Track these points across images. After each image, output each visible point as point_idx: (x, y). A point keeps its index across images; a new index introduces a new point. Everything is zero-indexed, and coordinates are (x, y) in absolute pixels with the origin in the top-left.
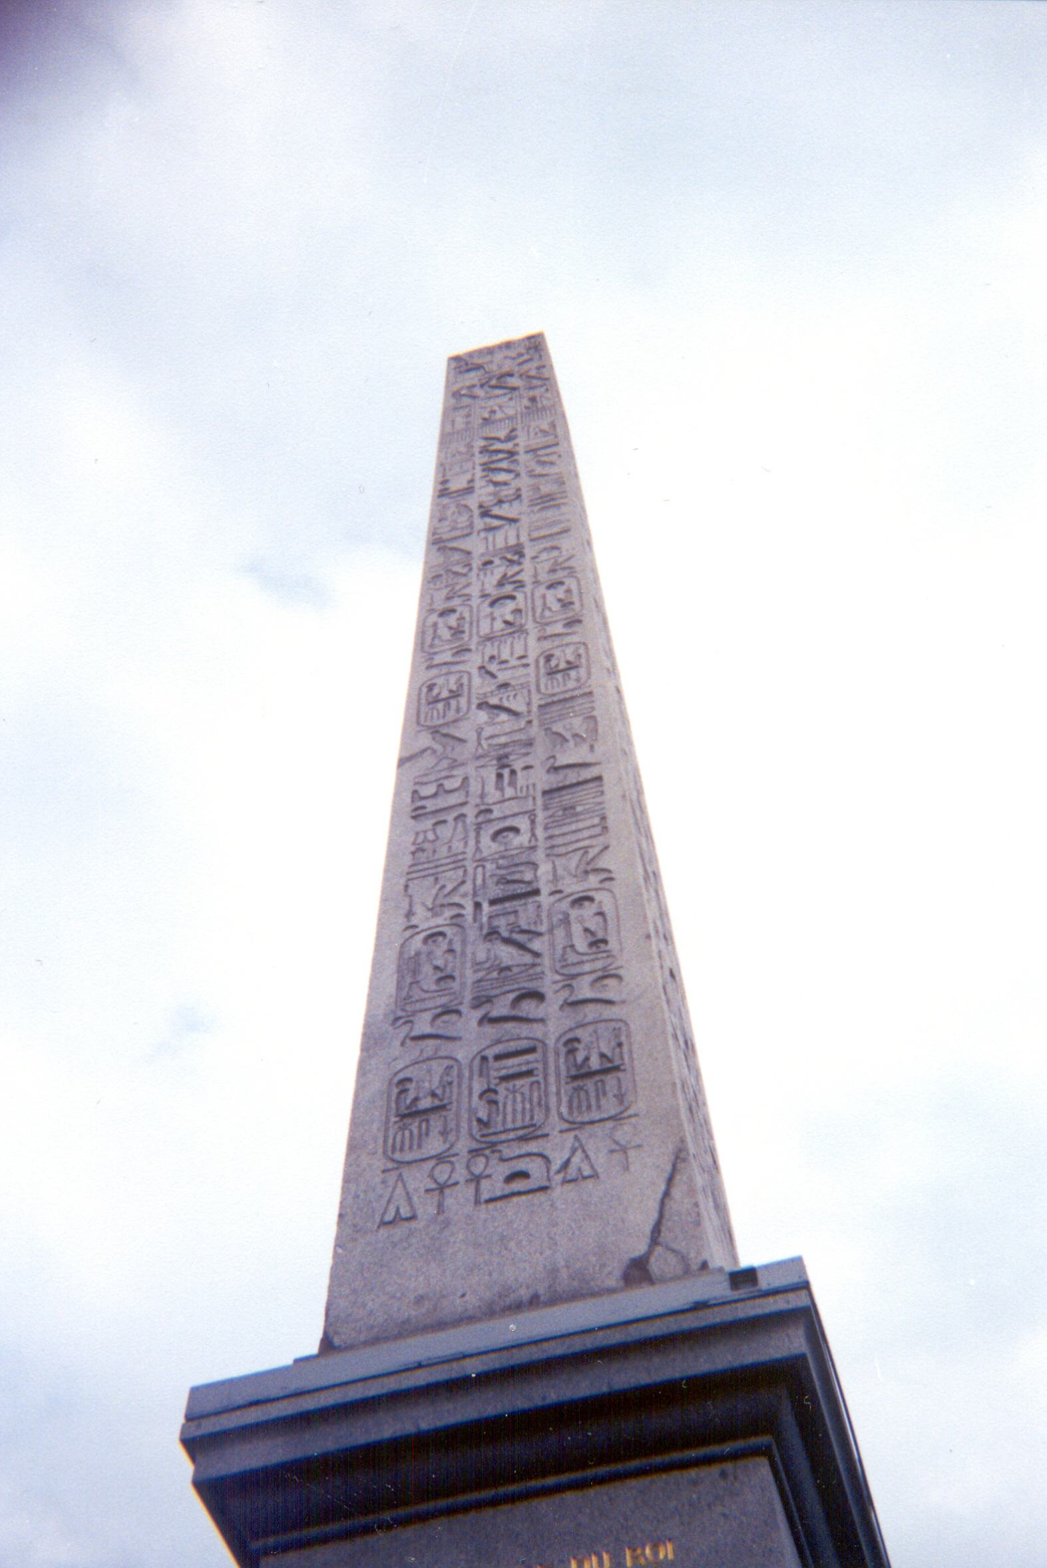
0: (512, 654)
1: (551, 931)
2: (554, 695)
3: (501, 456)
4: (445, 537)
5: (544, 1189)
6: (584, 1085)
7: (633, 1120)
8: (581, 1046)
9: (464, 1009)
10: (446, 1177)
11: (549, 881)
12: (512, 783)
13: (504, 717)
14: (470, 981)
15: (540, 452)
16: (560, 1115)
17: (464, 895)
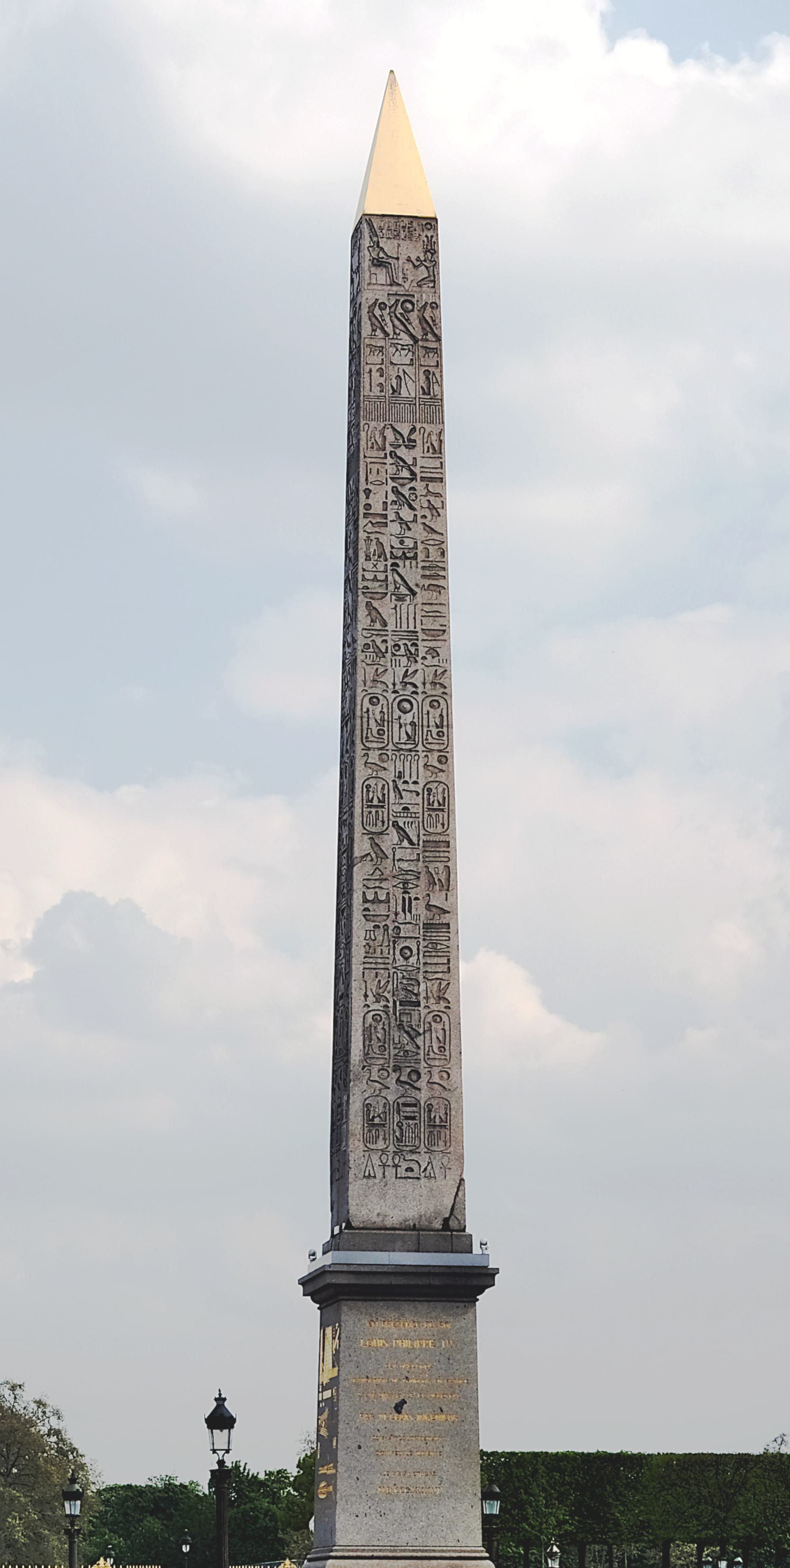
7: (449, 1155)
9: (390, 1070)
11: (424, 998)
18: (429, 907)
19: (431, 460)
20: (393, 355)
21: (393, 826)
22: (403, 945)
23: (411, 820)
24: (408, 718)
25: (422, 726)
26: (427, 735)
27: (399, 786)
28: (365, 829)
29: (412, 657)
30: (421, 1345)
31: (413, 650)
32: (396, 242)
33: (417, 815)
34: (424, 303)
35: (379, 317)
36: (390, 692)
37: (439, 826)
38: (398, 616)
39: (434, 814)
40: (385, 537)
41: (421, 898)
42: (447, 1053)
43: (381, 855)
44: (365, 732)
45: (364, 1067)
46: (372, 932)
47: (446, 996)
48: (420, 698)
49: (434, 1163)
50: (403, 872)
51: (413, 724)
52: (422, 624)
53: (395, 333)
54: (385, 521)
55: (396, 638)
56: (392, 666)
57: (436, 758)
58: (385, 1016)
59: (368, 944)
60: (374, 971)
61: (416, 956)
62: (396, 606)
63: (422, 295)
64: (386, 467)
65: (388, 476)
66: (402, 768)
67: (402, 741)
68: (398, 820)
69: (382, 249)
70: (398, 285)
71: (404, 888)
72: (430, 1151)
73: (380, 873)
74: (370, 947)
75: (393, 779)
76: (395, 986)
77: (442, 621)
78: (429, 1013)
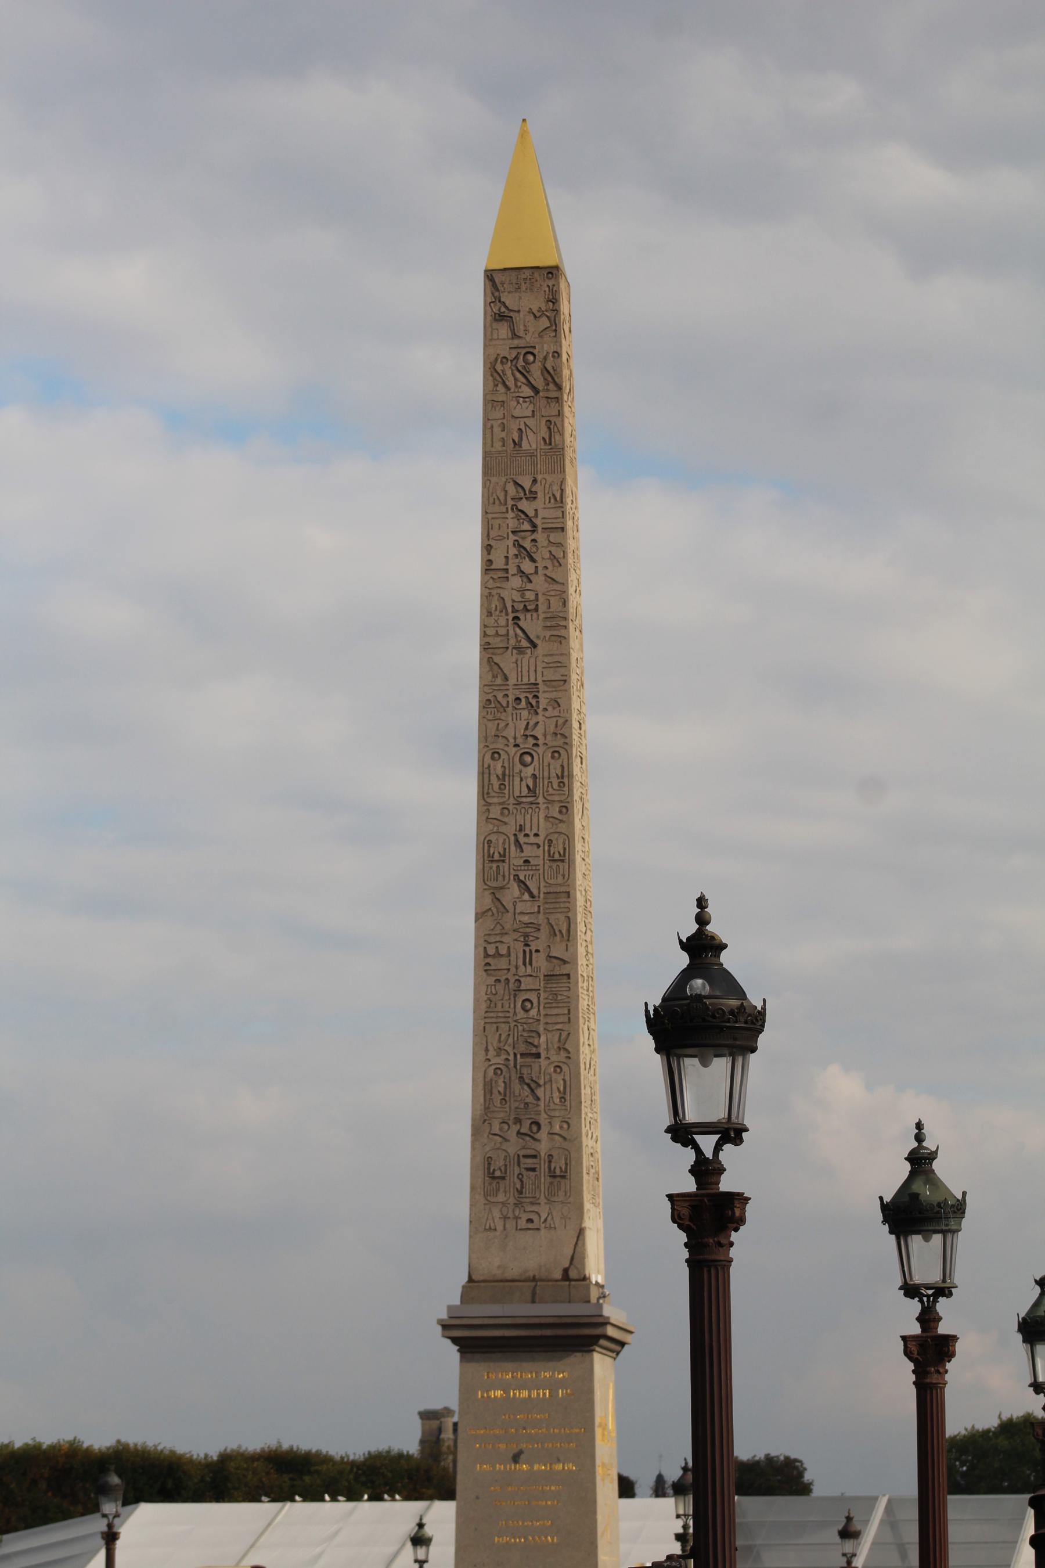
5: (538, 1229)
7: (569, 1205)
9: (510, 1123)
11: (545, 1049)
14: (513, 1108)
18: (550, 957)
19: (552, 510)
20: (515, 408)
21: (515, 879)
22: (524, 998)
23: (531, 873)
24: (529, 771)
25: (543, 778)
26: (548, 786)
27: (520, 840)
28: (486, 884)
29: (533, 709)
30: (538, 1394)
31: (534, 702)
32: (517, 295)
33: (538, 868)
34: (545, 353)
35: (500, 372)
36: (511, 745)
37: (560, 877)
38: (519, 670)
39: (554, 865)
40: (506, 593)
41: (541, 951)
42: (568, 1103)
43: (502, 909)
44: (486, 788)
45: (485, 1121)
46: (493, 987)
47: (566, 1046)
48: (541, 750)
49: (554, 1214)
50: (524, 926)
51: (534, 776)
52: (542, 676)
53: (516, 386)
54: (506, 575)
55: (517, 692)
56: (513, 720)
57: (557, 809)
58: (506, 1070)
59: (489, 999)
61: (537, 1007)
62: (517, 661)
63: (543, 346)
64: (508, 521)
65: (509, 530)
66: (523, 821)
67: (522, 795)
68: (519, 874)
69: (504, 304)
70: (520, 337)
71: (525, 941)
72: (549, 1201)
73: (501, 928)
74: (491, 1001)
75: (514, 832)
76: (516, 1039)
77: (563, 671)
78: (549, 1064)
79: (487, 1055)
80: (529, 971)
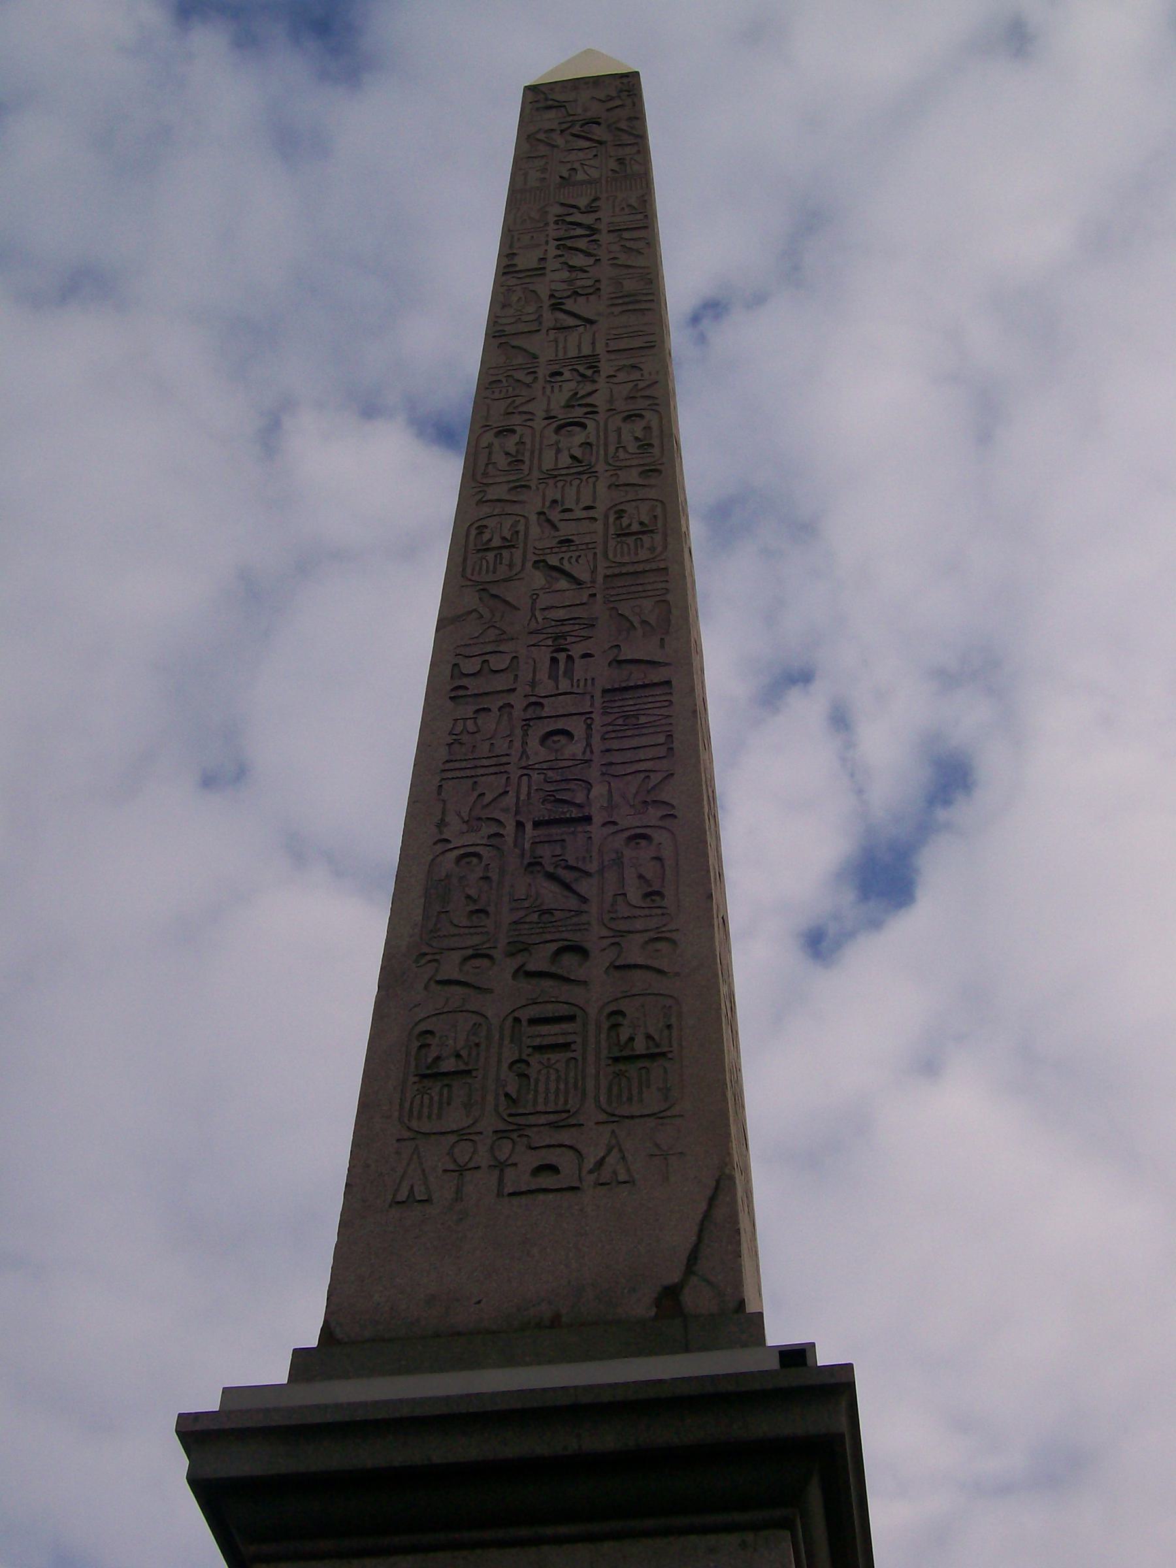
0: (578, 501)
1: (602, 871)
2: (624, 564)
3: (579, 231)
4: (509, 329)
6: (626, 1071)
8: (625, 1022)
9: (497, 954)
10: (467, 1158)
12: (569, 673)
13: (563, 584)
15: (627, 235)
16: (599, 1106)
17: (506, 810)
23: (577, 553)
50: (553, 623)
60: (471, 781)
79: (441, 833)
80: (564, 685)
